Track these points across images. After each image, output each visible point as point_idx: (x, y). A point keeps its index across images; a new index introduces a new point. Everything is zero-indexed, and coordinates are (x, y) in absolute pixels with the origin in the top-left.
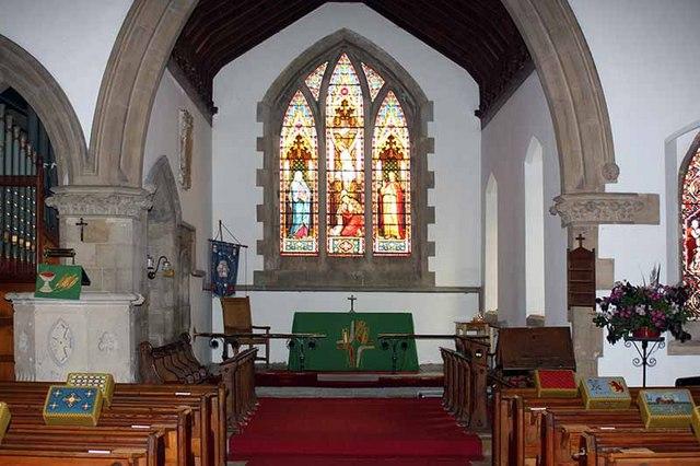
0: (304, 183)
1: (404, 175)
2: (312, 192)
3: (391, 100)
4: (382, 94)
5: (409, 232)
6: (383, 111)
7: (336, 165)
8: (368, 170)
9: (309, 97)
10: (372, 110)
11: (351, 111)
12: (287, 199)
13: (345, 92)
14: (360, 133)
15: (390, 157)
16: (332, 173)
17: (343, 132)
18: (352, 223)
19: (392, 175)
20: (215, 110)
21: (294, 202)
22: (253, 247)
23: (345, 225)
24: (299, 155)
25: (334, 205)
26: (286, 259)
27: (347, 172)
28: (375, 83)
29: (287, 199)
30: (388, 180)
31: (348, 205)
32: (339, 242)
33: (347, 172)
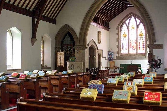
9: (126, 25)
10: (138, 26)
14: (136, 31)
15: (141, 35)
18: (134, 47)
20: (109, 28)
22: (116, 52)
26: (122, 55)
28: (138, 21)
30: (140, 39)
32: (132, 51)
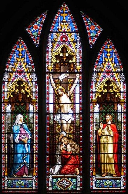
0: (25, 126)
1: (120, 117)
2: (32, 133)
3: (109, 47)
4: (100, 41)
5: (124, 172)
6: (101, 56)
7: (55, 108)
8: (86, 112)
10: (90, 56)
11: (70, 57)
12: (9, 140)
13: (64, 40)
15: (108, 101)
16: (52, 116)
17: (62, 77)
18: (71, 162)
19: (108, 117)
21: (15, 144)
23: (63, 164)
24: (20, 99)
25: (54, 145)
27: (66, 111)
29: (9, 140)
30: (105, 122)
31: (68, 146)
33: (66, 111)
